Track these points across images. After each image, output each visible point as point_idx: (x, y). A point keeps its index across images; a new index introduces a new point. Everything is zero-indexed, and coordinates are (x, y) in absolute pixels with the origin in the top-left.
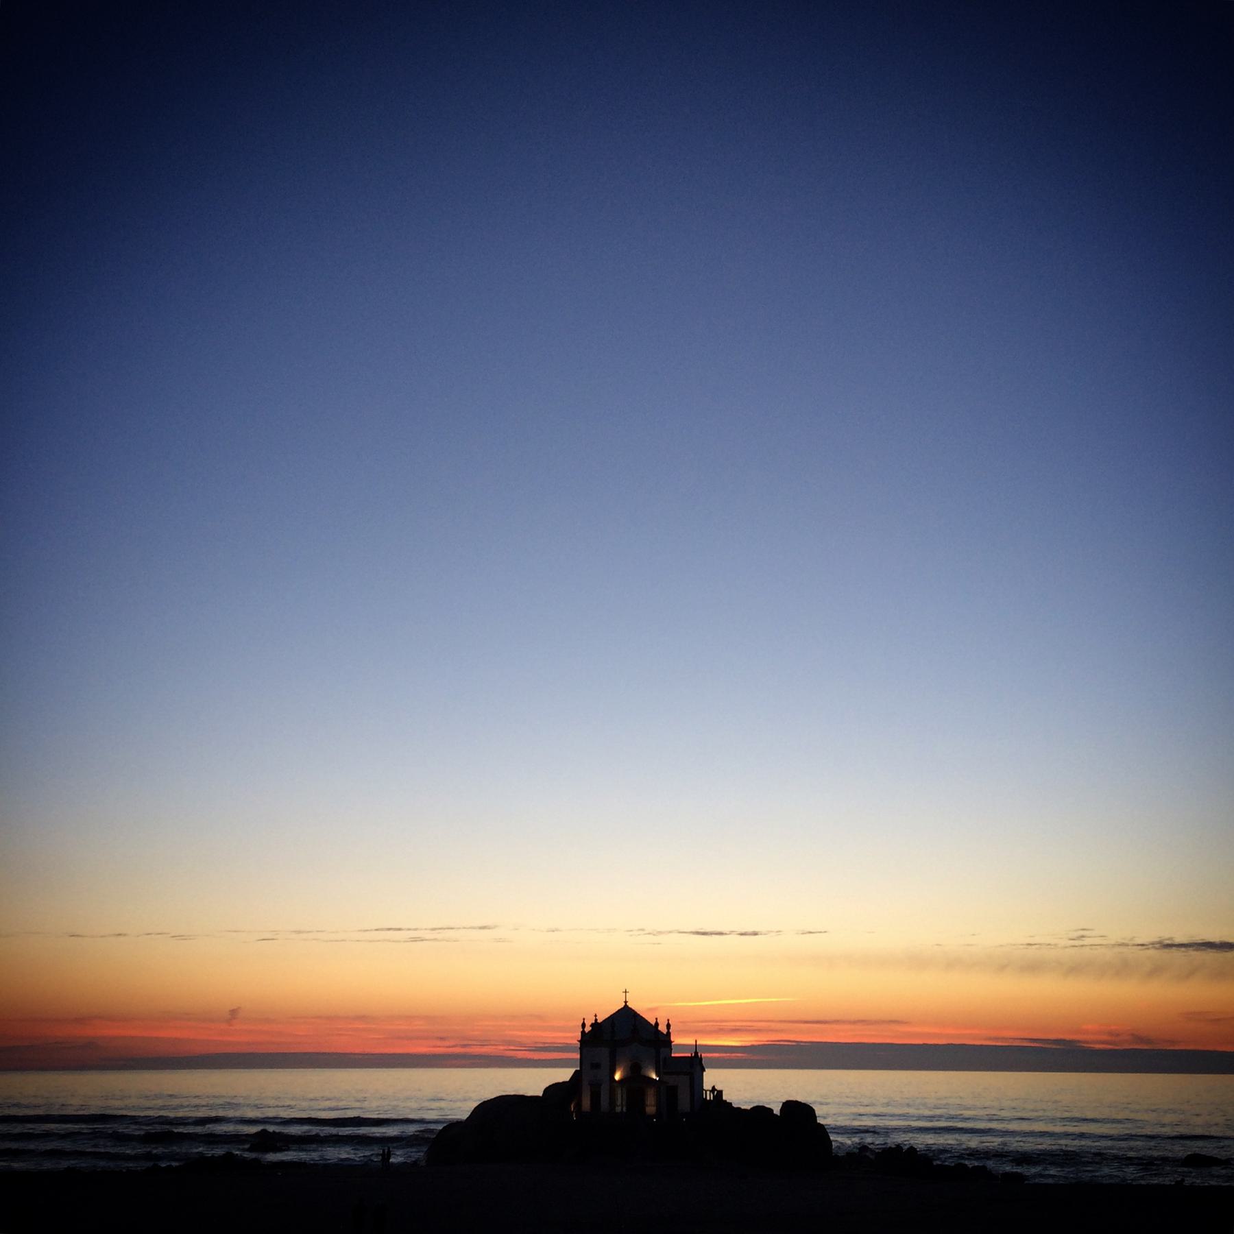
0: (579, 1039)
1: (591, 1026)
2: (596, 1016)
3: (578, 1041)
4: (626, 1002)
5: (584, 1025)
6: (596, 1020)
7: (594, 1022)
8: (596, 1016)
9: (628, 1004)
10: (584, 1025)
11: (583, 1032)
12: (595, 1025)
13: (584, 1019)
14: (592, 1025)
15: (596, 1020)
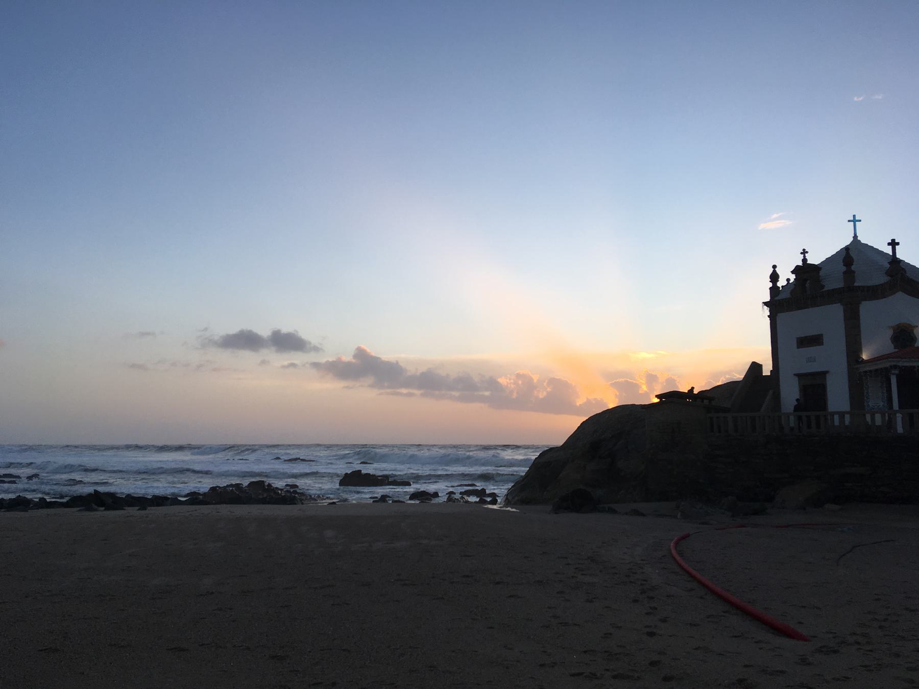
0: (767, 298)
1: (793, 272)
2: (804, 252)
3: (765, 304)
4: (855, 237)
5: (774, 277)
6: (805, 260)
7: (800, 263)
8: (804, 252)
9: (859, 239)
10: (774, 277)
11: (774, 290)
12: (804, 271)
13: (774, 267)
14: (796, 271)
15: (805, 260)
